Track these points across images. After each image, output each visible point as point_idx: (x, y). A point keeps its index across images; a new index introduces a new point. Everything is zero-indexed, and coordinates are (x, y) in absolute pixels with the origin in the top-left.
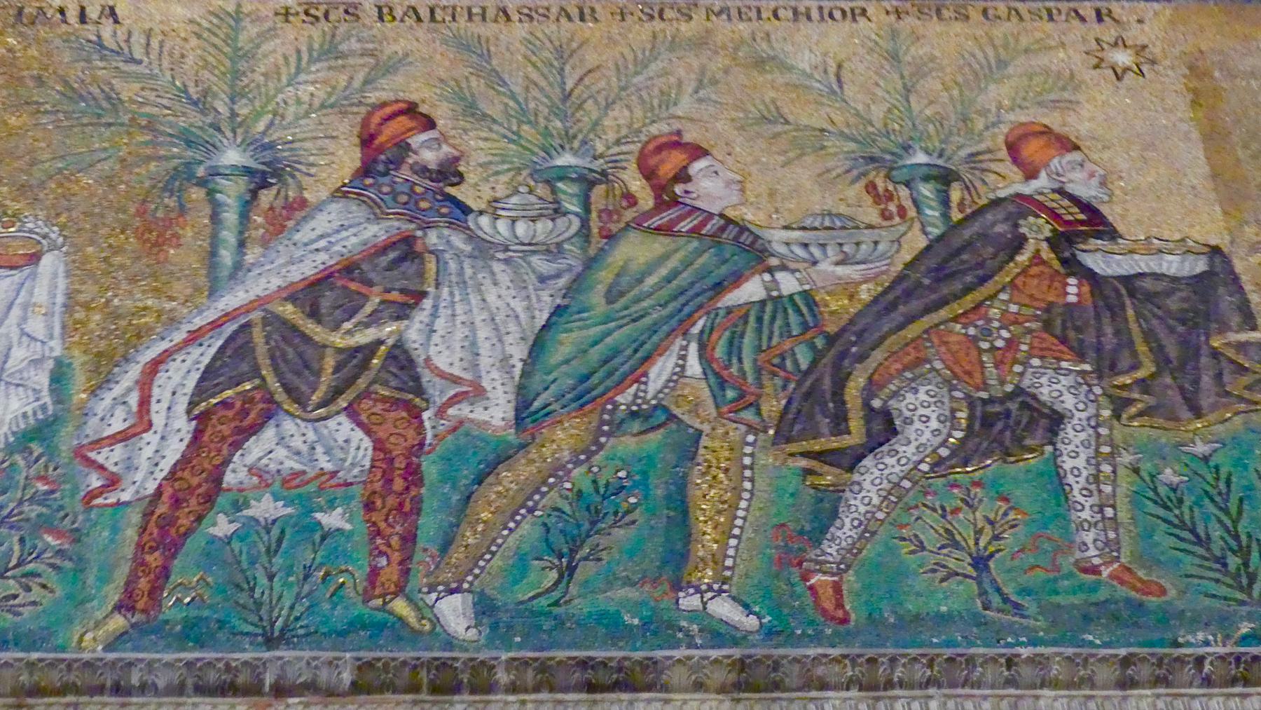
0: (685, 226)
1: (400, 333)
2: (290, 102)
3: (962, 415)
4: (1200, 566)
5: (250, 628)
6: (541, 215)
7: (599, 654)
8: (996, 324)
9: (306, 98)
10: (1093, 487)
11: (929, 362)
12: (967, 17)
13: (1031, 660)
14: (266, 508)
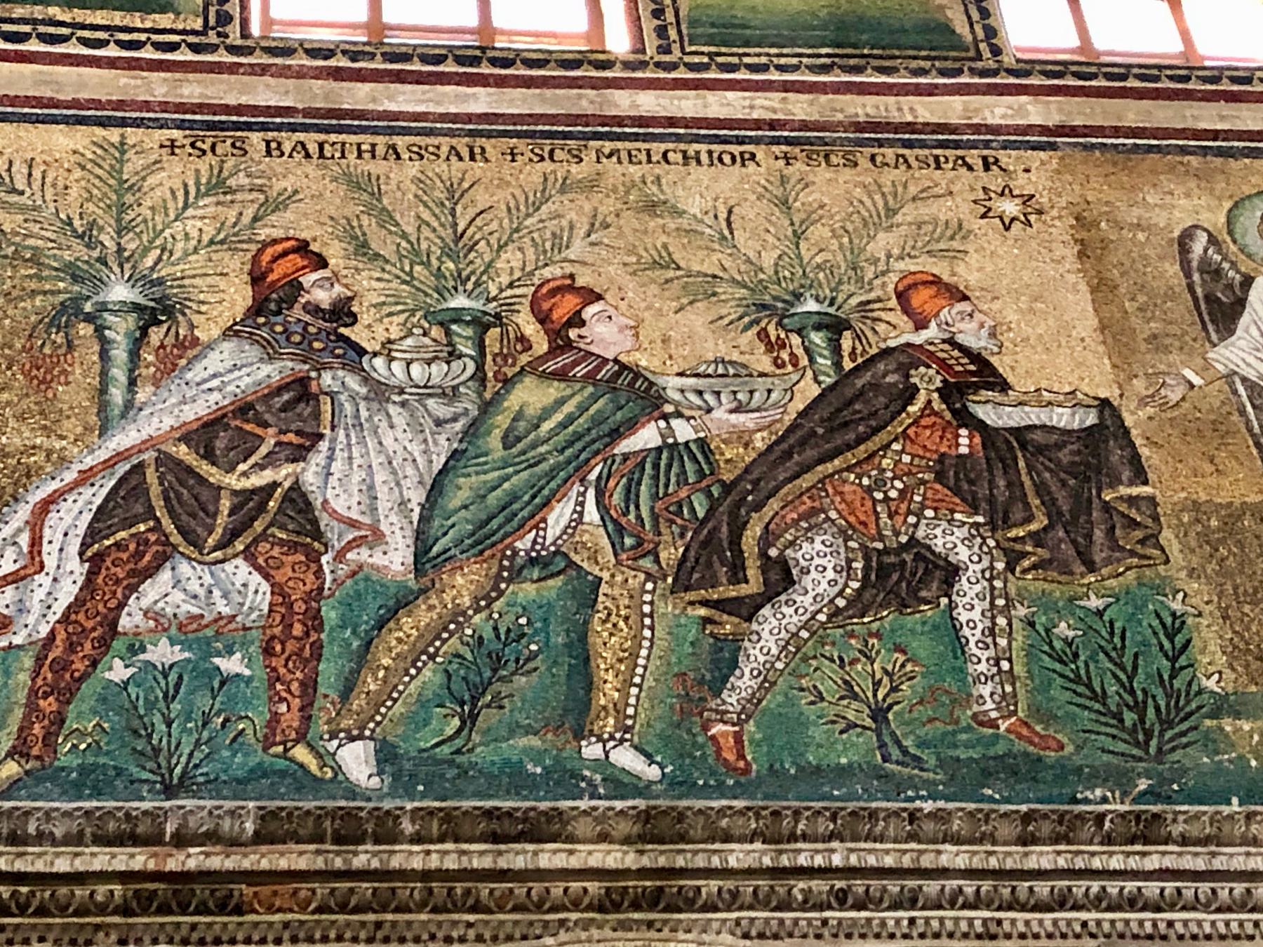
0: (580, 371)
3: (858, 565)
5: (145, 775)
6: (436, 358)
7: (507, 804)
8: (889, 474)
9: (195, 234)
10: (989, 640)
11: (825, 512)
12: (856, 164)
13: (933, 815)
14: (163, 652)
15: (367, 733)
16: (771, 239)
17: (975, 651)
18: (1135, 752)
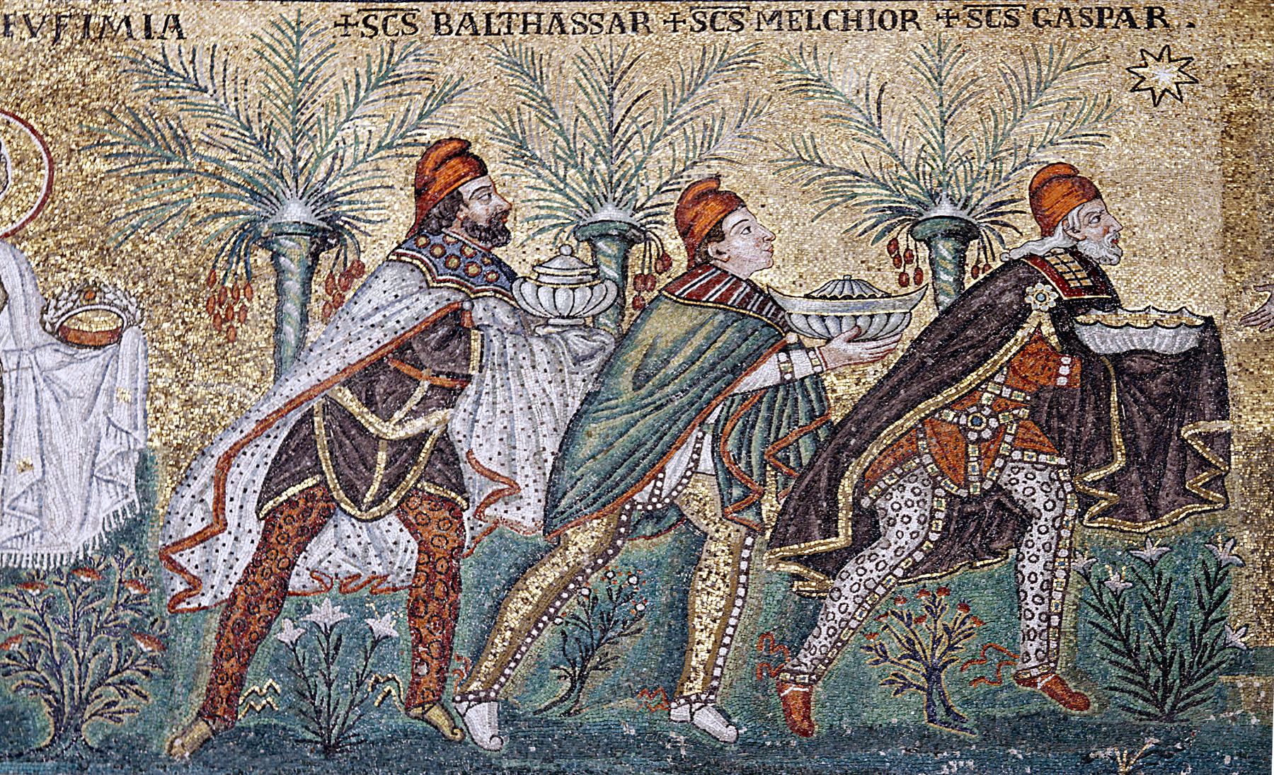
1: (445, 423)
2: (350, 141)
4: (1125, 678)
6: (581, 282)
11: (920, 456)
12: (1017, 23)
14: (326, 612)
15: (493, 694)
16: (918, 124)
17: (1032, 606)
18: (1151, 709)
